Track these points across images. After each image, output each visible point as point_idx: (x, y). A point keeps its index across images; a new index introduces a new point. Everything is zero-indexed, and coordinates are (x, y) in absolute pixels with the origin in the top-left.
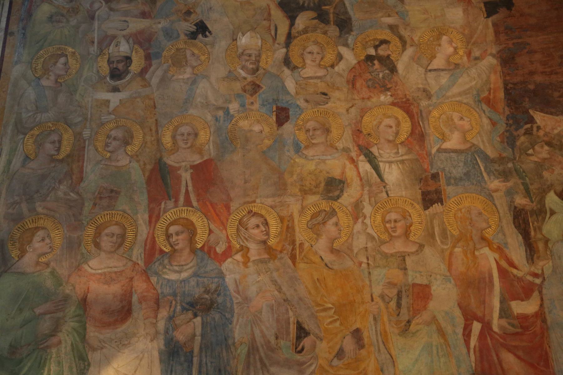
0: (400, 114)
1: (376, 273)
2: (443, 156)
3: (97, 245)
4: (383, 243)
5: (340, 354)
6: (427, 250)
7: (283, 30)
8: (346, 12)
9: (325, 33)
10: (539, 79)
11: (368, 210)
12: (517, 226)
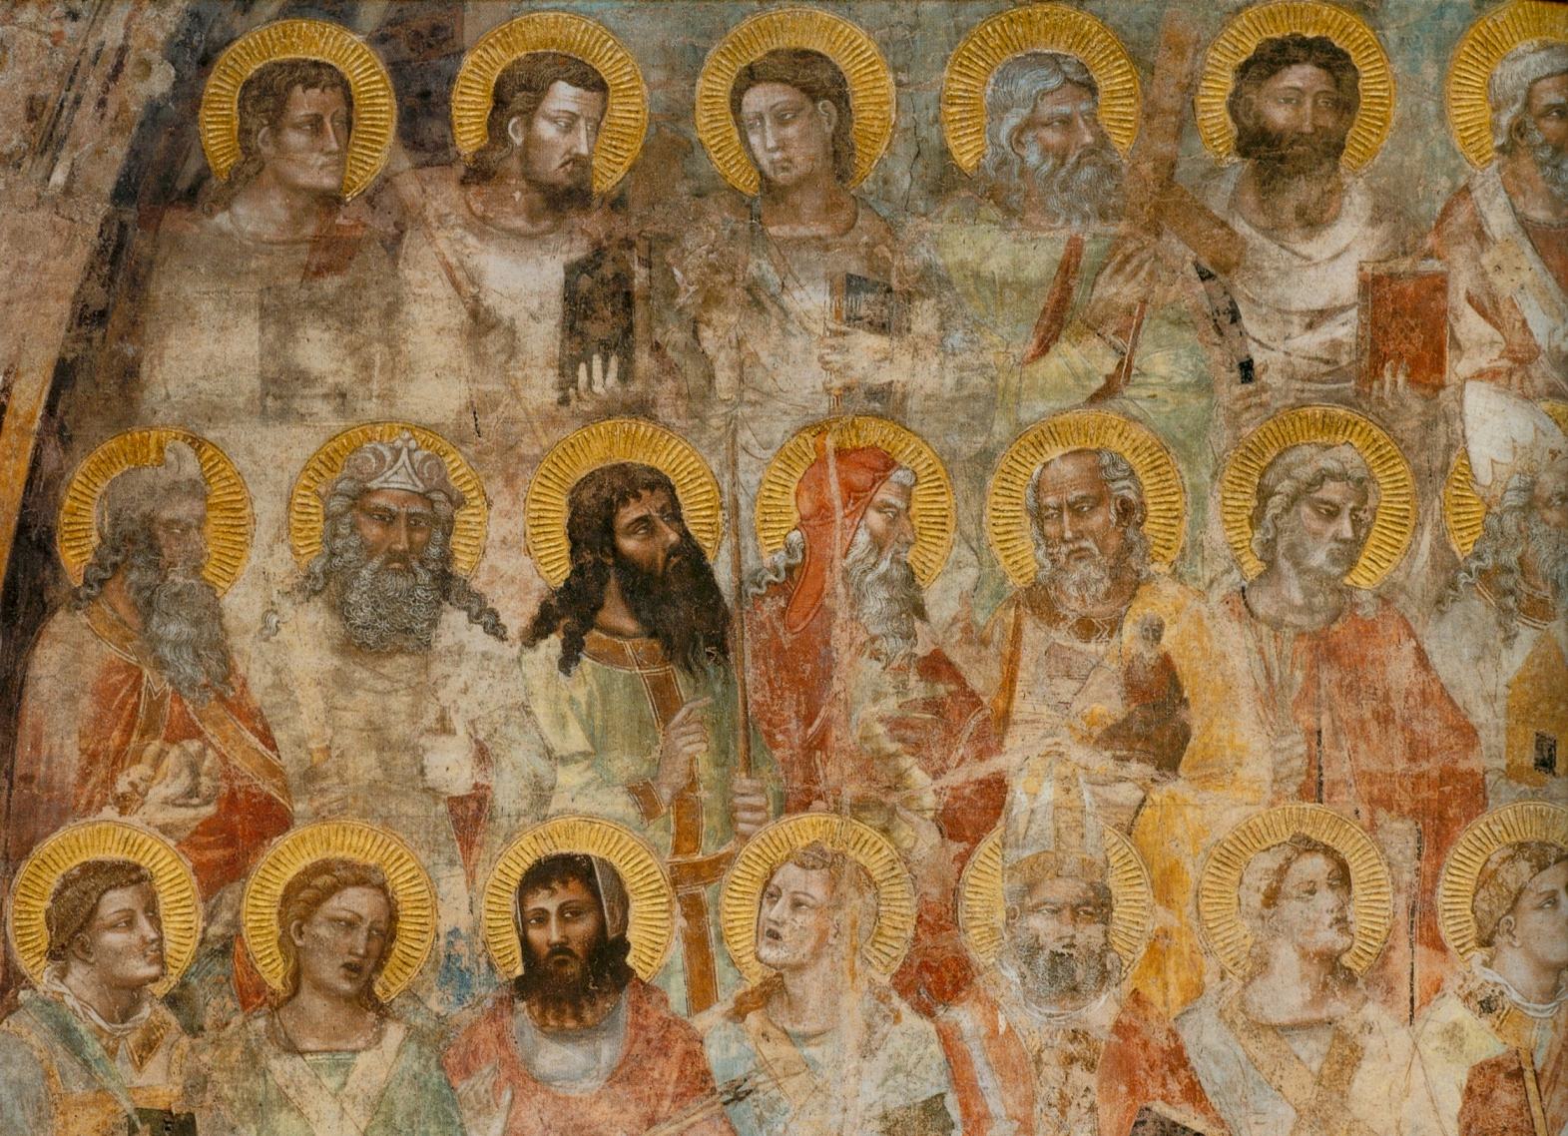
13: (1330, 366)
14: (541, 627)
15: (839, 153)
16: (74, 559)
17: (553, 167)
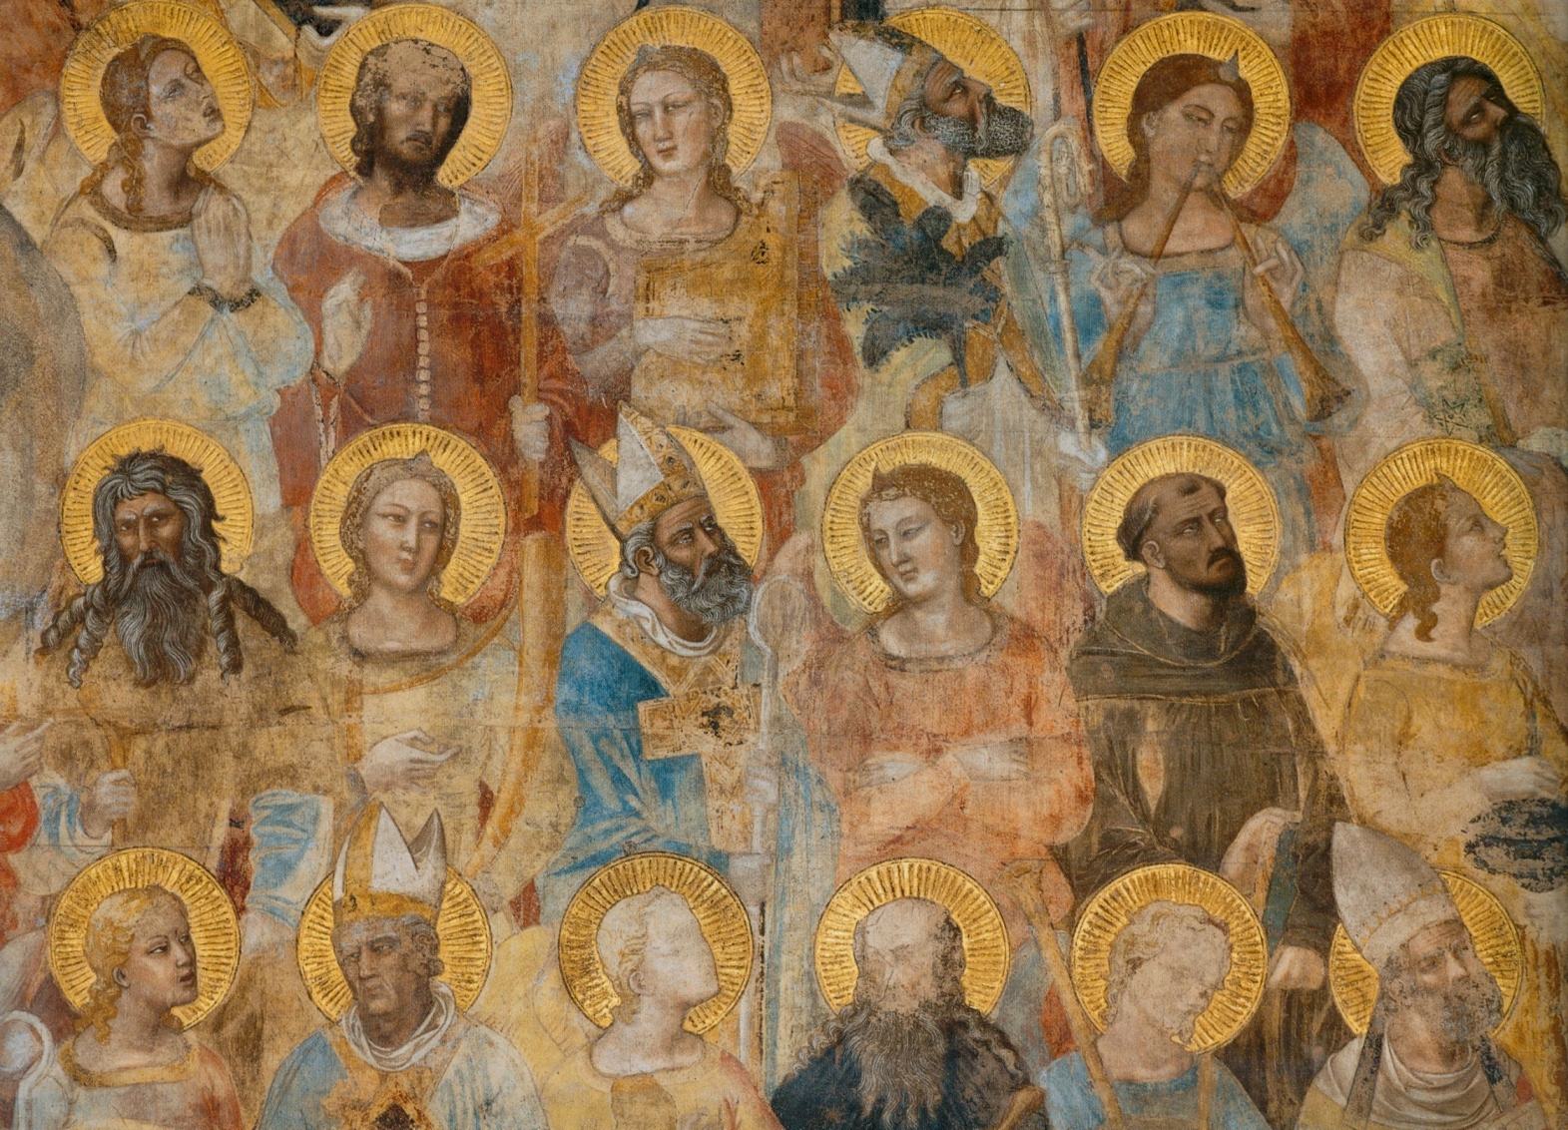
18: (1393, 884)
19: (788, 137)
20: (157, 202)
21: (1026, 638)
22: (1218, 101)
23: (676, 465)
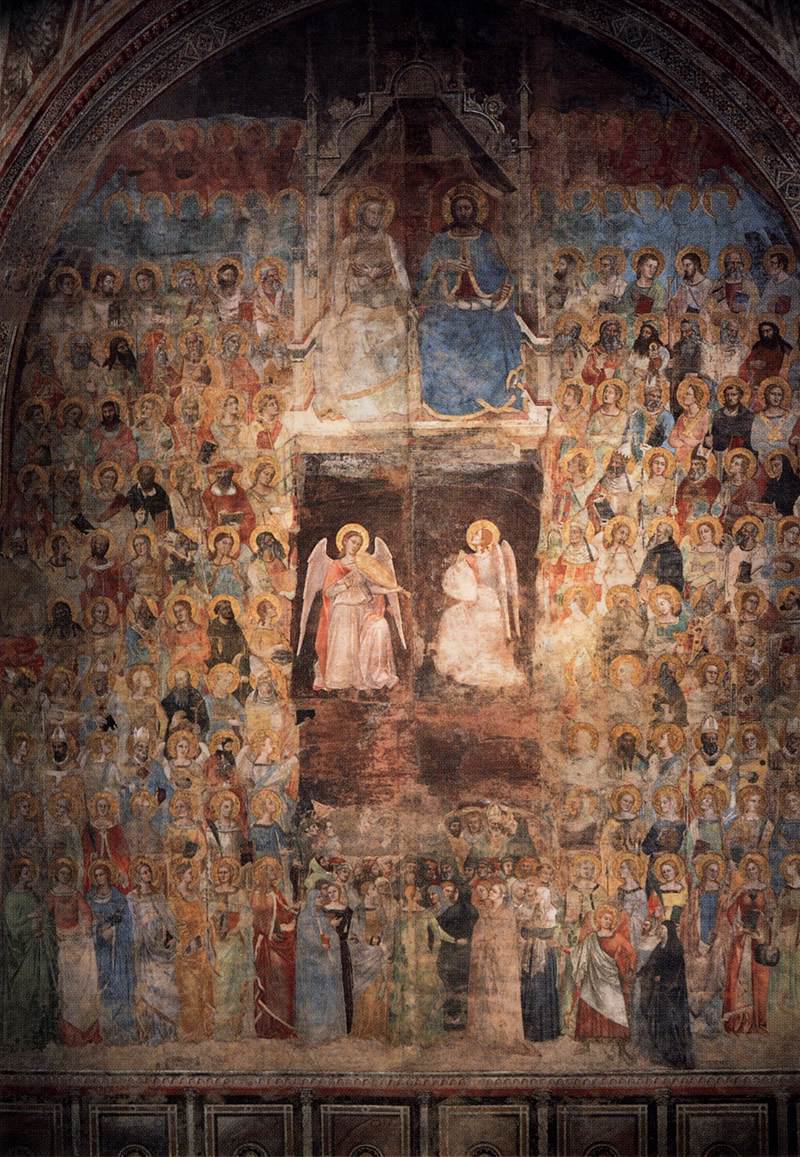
0: (234, 797)
1: (211, 904)
2: (257, 829)
3: (57, 880)
4: (217, 886)
5: (189, 949)
6: (241, 891)
7: (164, 727)
8: (206, 714)
9: (191, 730)
10: (321, 776)
11: (209, 865)
12: (291, 879)
13: (233, 318)
14: (105, 365)
15: (154, 286)
16: (29, 355)
17: (107, 289)
18: (260, 665)
19: (159, 548)
20: (60, 562)
21: (200, 627)
22: (228, 540)
23: (143, 601)
